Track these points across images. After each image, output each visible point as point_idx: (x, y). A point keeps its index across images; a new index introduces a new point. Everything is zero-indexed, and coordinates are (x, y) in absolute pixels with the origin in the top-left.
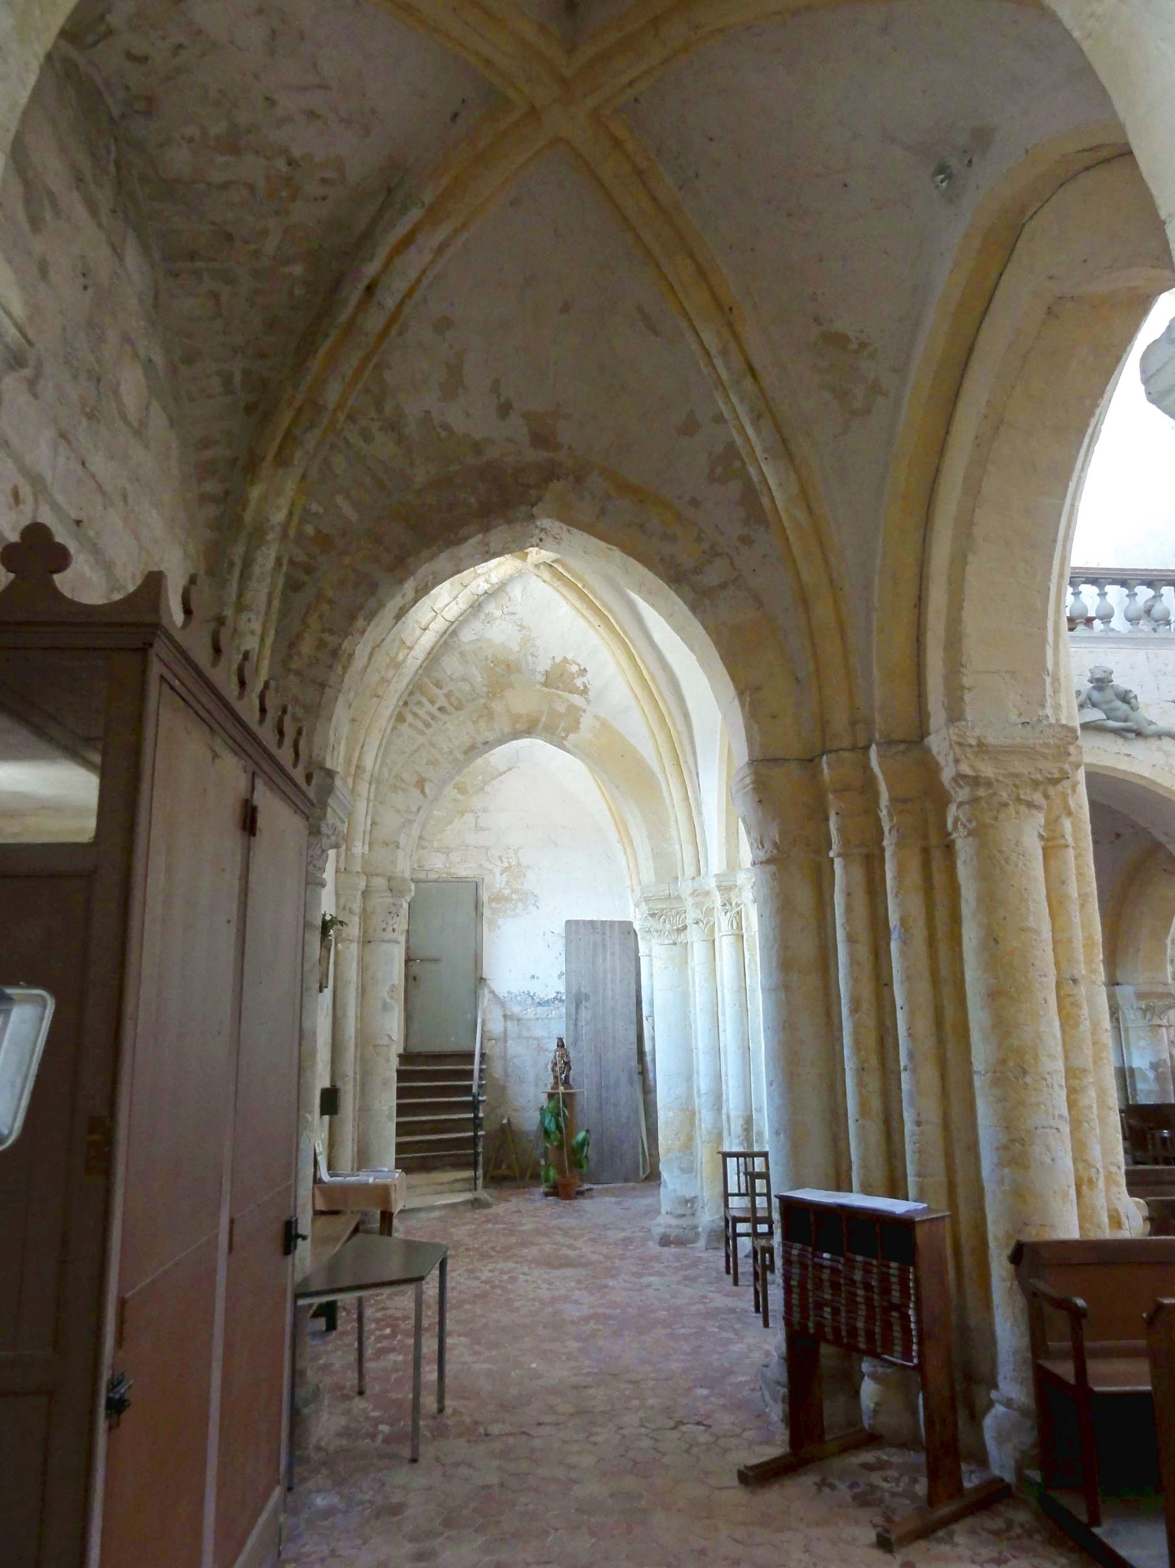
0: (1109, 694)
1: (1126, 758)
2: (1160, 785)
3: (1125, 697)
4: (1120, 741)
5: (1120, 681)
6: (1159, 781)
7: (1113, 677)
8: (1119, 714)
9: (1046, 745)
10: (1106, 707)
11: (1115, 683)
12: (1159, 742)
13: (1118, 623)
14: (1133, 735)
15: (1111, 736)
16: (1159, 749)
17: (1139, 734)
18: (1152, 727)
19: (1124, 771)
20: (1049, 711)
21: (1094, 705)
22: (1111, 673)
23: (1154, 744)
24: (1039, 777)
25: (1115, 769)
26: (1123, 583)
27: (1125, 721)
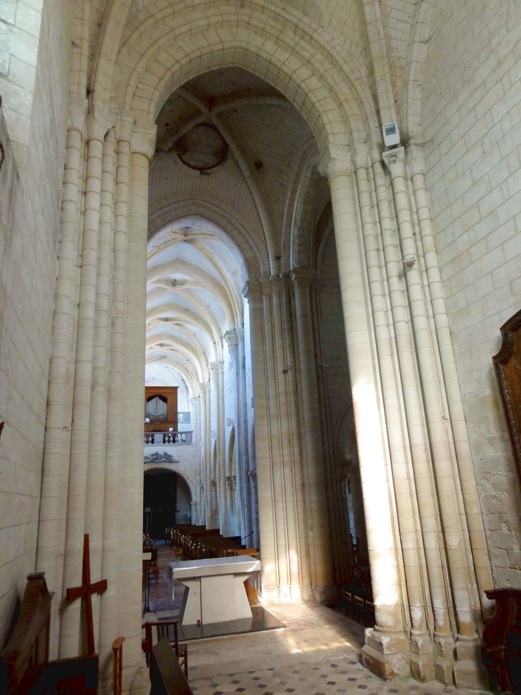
3: (170, 456)
5: (169, 453)
17: (172, 462)
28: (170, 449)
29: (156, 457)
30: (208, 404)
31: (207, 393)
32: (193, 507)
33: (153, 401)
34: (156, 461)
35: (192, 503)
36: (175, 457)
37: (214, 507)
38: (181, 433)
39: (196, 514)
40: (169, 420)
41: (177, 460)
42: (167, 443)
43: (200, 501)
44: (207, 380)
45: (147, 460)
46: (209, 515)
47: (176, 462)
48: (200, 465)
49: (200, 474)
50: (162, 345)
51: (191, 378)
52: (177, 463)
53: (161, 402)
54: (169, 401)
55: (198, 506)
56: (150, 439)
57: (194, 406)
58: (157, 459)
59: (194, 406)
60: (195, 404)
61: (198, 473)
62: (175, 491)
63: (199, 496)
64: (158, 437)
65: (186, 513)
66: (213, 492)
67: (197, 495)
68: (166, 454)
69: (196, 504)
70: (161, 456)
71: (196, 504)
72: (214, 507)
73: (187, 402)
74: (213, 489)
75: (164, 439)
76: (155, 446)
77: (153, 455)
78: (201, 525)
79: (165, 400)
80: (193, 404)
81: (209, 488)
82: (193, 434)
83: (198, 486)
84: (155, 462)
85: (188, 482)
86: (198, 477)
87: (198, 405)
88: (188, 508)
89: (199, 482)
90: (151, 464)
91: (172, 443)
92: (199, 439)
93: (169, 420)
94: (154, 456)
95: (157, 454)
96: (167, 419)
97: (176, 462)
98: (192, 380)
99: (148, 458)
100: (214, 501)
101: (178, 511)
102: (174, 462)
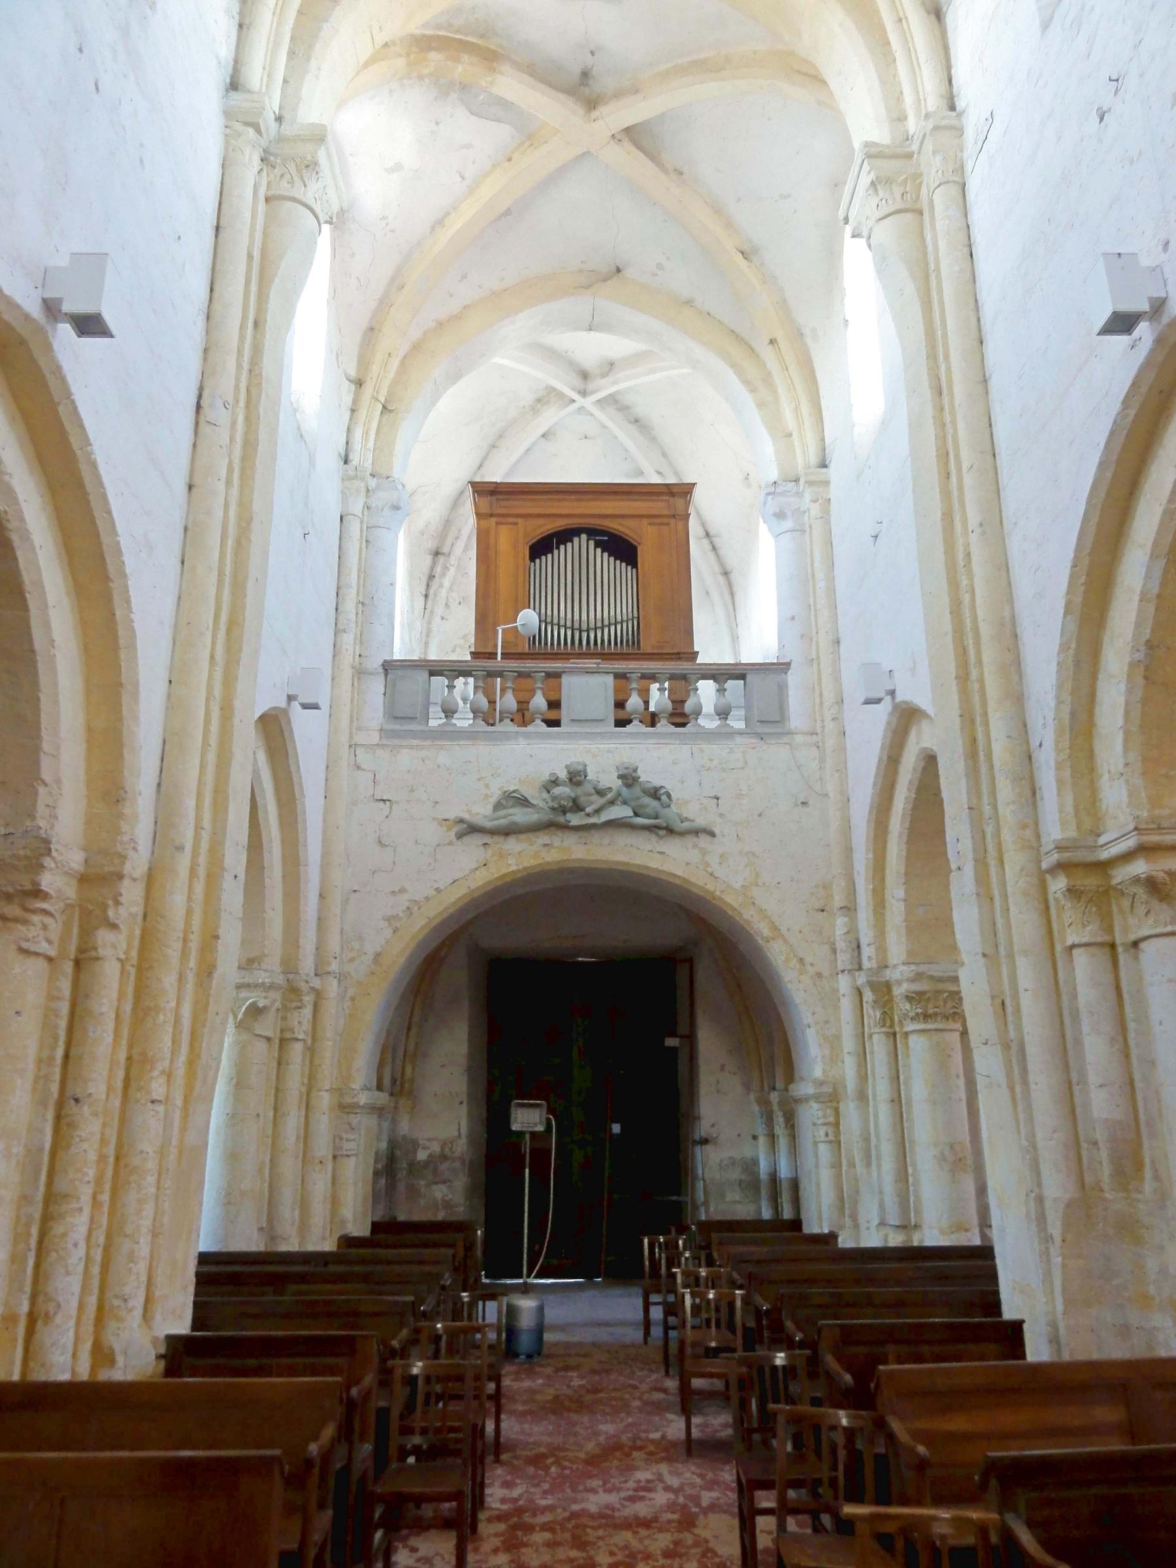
0: (637, 791)
1: (658, 856)
2: (696, 885)
3: (655, 793)
4: (654, 838)
5: (649, 776)
6: (693, 880)
7: (639, 772)
8: (648, 810)
9: (14, 856)
10: (633, 803)
11: (643, 778)
12: (695, 839)
13: (464, 720)
14: (662, 832)
15: (646, 834)
16: (695, 846)
17: (670, 831)
18: (686, 825)
19: (657, 870)
20: (42, 823)
21: (625, 803)
22: (635, 770)
23: (690, 840)
24: (11, 890)
25: (647, 868)
26: (713, 677)
27: (656, 818)
28: (657, 757)
29: (569, 805)
30: (948, 265)
31: (942, 202)
32: (811, 1116)
33: (565, 554)
34: (575, 820)
35: (804, 1089)
36: (689, 801)
37: (1101, 1104)
38: (720, 675)
39: (836, 1165)
40: (647, 646)
41: (700, 822)
42: (635, 727)
43: (863, 1077)
44: (933, 102)
45: (520, 816)
46: (1057, 1187)
47: (696, 832)
48: (848, 851)
49: (850, 909)
50: (583, 88)
51: (768, 379)
52: (703, 840)
53: (603, 562)
54: (643, 555)
55: (850, 1110)
56: (539, 702)
57: (789, 524)
58: (577, 807)
59: (789, 524)
60: (799, 513)
61: (838, 900)
62: (691, 1038)
63: (848, 1043)
64: (589, 690)
65: (747, 1151)
66: (1084, 969)
67: (833, 1042)
68: (629, 778)
69: (832, 1098)
70: (600, 793)
71: (832, 1098)
72: (1101, 1104)
73: (727, 640)
74: (1075, 929)
75: (620, 705)
76: (570, 736)
77: (555, 782)
78: (872, 1239)
79: (622, 549)
80: (780, 515)
81: (1023, 923)
82: (793, 679)
83: (844, 984)
84: (565, 827)
85: (777, 955)
86: (841, 922)
87: (815, 510)
88: (761, 1130)
89: (843, 960)
90: (543, 838)
91: (663, 726)
92: (829, 696)
93: (647, 646)
94: (563, 791)
95: (576, 777)
96: (636, 642)
97: (696, 832)
98: (775, 392)
99: (524, 802)
100: (1096, 1050)
101: (705, 1141)
102: (682, 834)
